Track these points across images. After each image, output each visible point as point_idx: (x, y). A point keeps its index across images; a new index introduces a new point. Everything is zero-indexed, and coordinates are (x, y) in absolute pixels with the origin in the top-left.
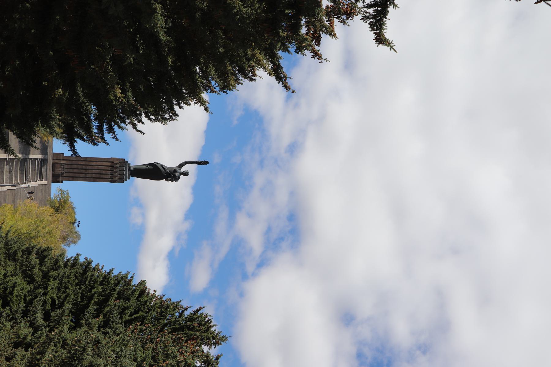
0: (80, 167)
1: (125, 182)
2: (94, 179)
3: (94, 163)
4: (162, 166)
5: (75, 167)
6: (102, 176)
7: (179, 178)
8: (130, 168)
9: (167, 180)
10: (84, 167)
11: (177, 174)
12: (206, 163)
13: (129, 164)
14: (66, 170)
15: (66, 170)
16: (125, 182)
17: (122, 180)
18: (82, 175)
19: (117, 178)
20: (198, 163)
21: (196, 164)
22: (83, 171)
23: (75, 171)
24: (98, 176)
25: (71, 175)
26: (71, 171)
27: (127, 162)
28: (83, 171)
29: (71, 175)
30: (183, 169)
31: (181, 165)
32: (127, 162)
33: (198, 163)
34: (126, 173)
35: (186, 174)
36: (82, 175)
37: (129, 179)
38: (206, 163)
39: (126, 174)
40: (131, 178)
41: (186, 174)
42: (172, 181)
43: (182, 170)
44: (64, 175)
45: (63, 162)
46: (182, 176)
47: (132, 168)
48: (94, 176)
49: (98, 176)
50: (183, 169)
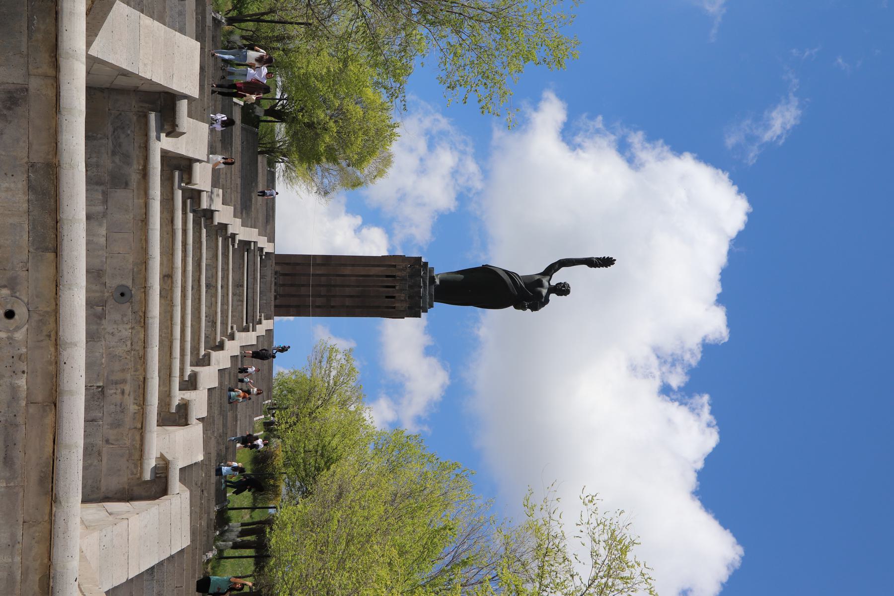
1: (423, 314)
3: (348, 271)
4: (506, 272)
7: (547, 301)
8: (432, 279)
9: (519, 306)
10: (323, 279)
11: (544, 292)
12: (607, 262)
13: (432, 269)
16: (423, 314)
18: (320, 301)
19: (405, 305)
20: (591, 263)
21: (585, 267)
22: (323, 291)
27: (426, 264)
28: (323, 291)
30: (557, 278)
31: (551, 270)
32: (426, 264)
33: (591, 263)
34: (426, 292)
35: (562, 290)
36: (320, 301)
37: (431, 306)
38: (607, 262)
39: (425, 295)
40: (435, 303)
42: (535, 308)
43: (553, 282)
46: (553, 297)
47: (438, 281)
48: (348, 302)
50: (557, 278)
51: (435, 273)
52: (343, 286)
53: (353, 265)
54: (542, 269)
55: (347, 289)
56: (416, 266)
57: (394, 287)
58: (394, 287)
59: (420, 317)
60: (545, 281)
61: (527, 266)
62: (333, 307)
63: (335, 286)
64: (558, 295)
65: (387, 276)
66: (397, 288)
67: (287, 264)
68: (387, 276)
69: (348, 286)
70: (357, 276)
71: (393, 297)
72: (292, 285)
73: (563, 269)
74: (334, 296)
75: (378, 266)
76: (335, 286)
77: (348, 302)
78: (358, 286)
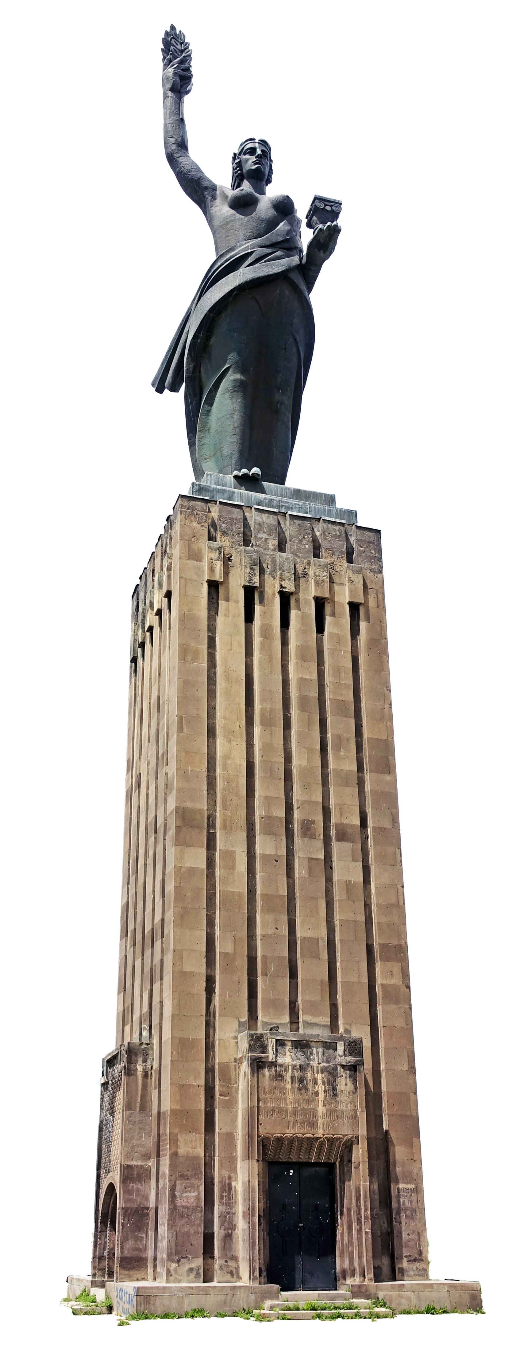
0: (270, 883)
2: (376, 757)
5: (268, 925)
6: (338, 690)
14: (314, 1024)
15: (314, 1024)
20: (180, 84)
22: (307, 850)
23: (310, 928)
24: (341, 726)
25: (351, 972)
26: (311, 971)
28: (307, 850)
29: (351, 972)
31: (196, 188)
33: (180, 84)
36: (346, 869)
45: (232, 1043)
48: (342, 762)
49: (341, 726)
65: (249, 617)
68: (249, 617)
69: (288, 758)
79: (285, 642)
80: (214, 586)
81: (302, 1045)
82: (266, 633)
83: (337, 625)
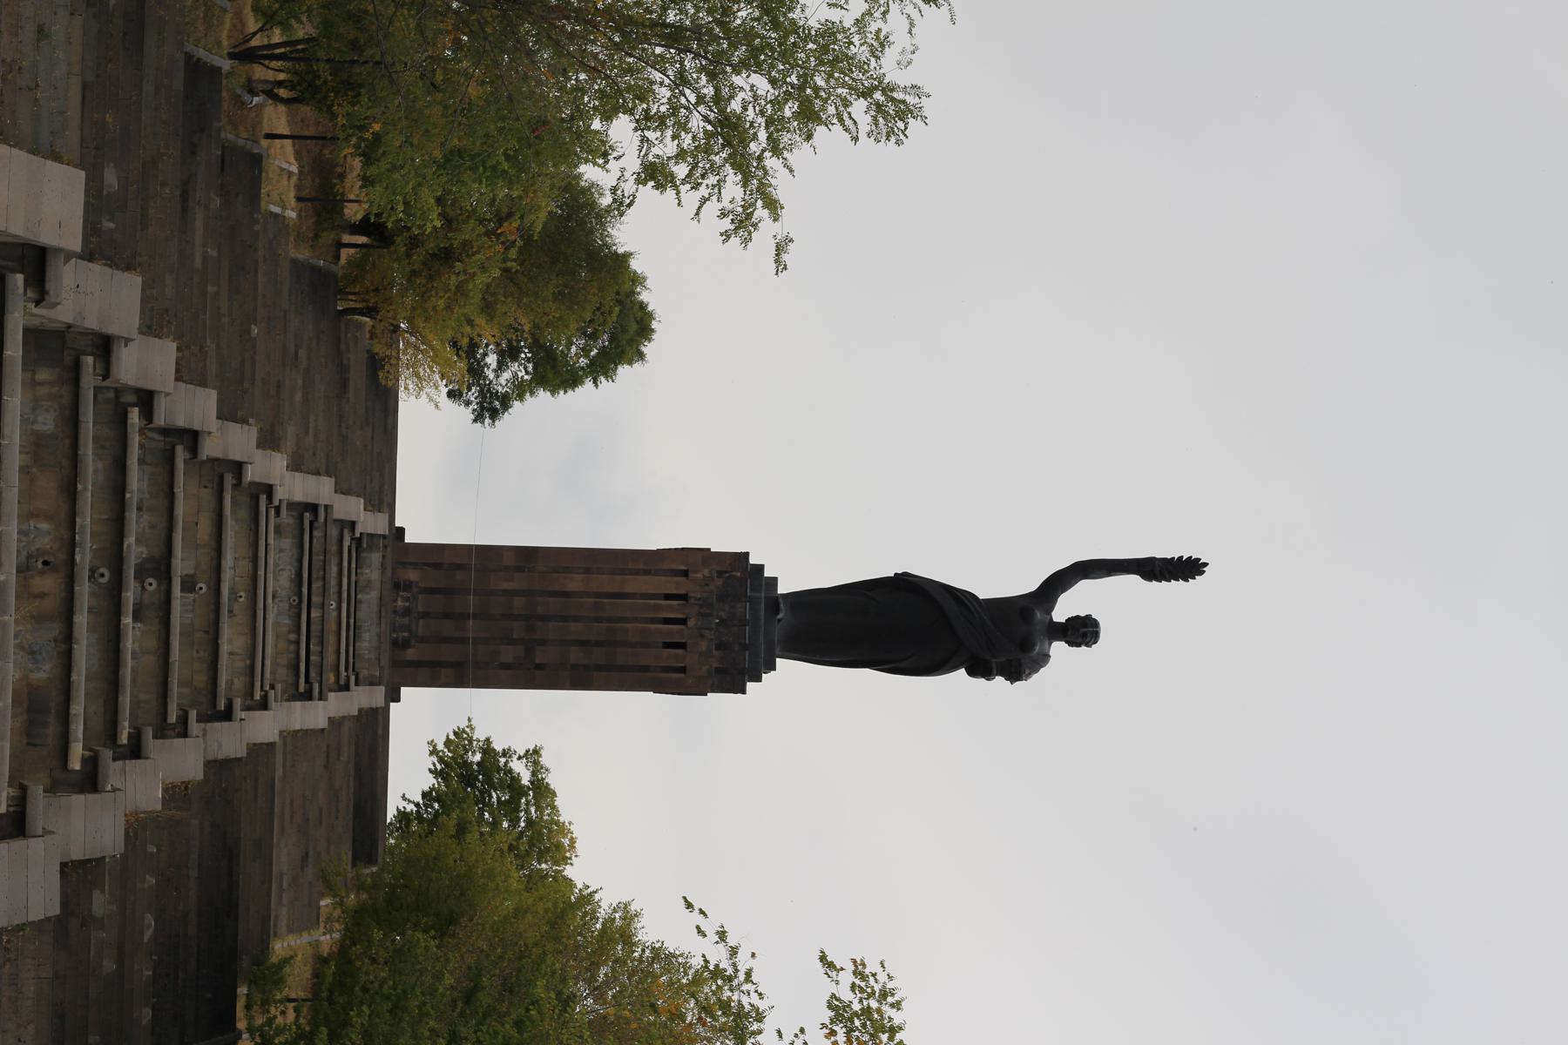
1: (750, 685)
3: (574, 583)
7: (1044, 659)
9: (980, 669)
10: (519, 602)
12: (1187, 569)
16: (750, 685)
17: (733, 675)
18: (508, 654)
21: (1135, 579)
27: (760, 568)
30: (1065, 608)
32: (760, 568)
35: (1083, 631)
36: (508, 654)
38: (1187, 569)
41: (1083, 631)
42: (1015, 673)
43: (1060, 614)
44: (411, 654)
46: (1058, 649)
48: (576, 655)
50: (1065, 608)
51: (783, 589)
52: (564, 619)
53: (588, 571)
54: (1031, 585)
55: (573, 626)
56: (738, 574)
57: (683, 622)
58: (683, 622)
59: (743, 692)
60: (1039, 615)
61: (996, 576)
62: (539, 667)
63: (545, 618)
64: (1071, 644)
65: (668, 597)
66: (691, 623)
67: (437, 566)
68: (668, 597)
69: (576, 619)
70: (599, 595)
71: (682, 646)
72: (446, 616)
73: (1084, 586)
74: (543, 642)
75: (647, 572)
76: (545, 618)
77: (576, 655)
78: (599, 620)
79: (653, 621)
80: (685, 573)
81: (407, 612)
82: (657, 608)
83: (669, 657)
